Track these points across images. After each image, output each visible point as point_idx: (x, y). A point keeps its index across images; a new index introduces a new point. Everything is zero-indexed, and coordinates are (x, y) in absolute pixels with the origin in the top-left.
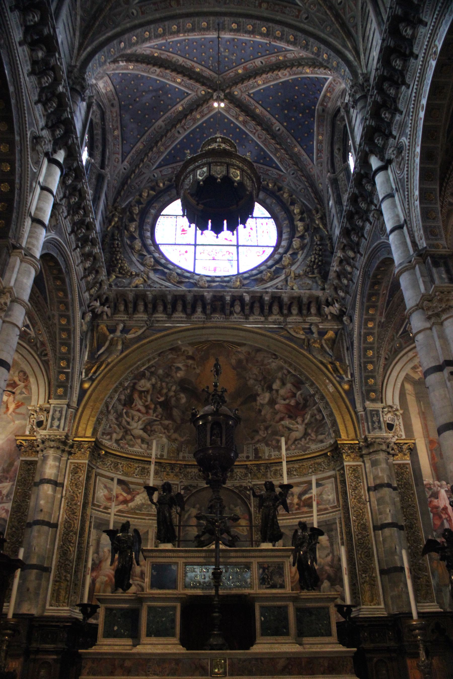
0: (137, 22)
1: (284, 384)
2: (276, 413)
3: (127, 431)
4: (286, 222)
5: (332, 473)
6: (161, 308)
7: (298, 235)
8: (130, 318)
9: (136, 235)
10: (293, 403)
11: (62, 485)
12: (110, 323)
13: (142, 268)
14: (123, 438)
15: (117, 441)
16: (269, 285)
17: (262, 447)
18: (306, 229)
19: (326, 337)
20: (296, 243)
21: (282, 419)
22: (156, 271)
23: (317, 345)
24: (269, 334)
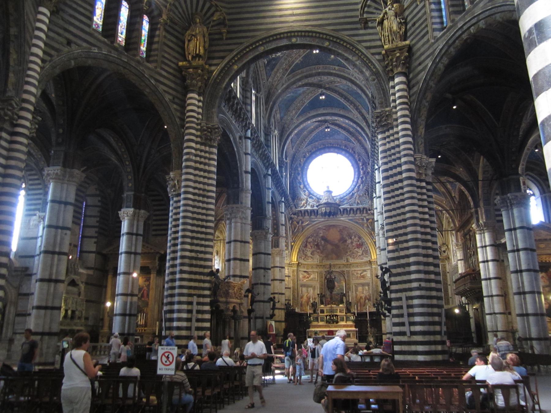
0: (296, 124)
1: (355, 237)
2: (353, 246)
3: (306, 255)
4: (357, 169)
5: (369, 268)
6: (313, 214)
7: (361, 176)
8: (303, 218)
9: (301, 181)
10: (358, 243)
11: (290, 276)
12: (296, 220)
13: (305, 197)
14: (305, 258)
15: (304, 259)
16: (350, 201)
17: (349, 257)
18: (364, 173)
19: (369, 221)
20: (359, 182)
21: (355, 248)
22: (310, 197)
23: (366, 225)
24: (350, 221)
